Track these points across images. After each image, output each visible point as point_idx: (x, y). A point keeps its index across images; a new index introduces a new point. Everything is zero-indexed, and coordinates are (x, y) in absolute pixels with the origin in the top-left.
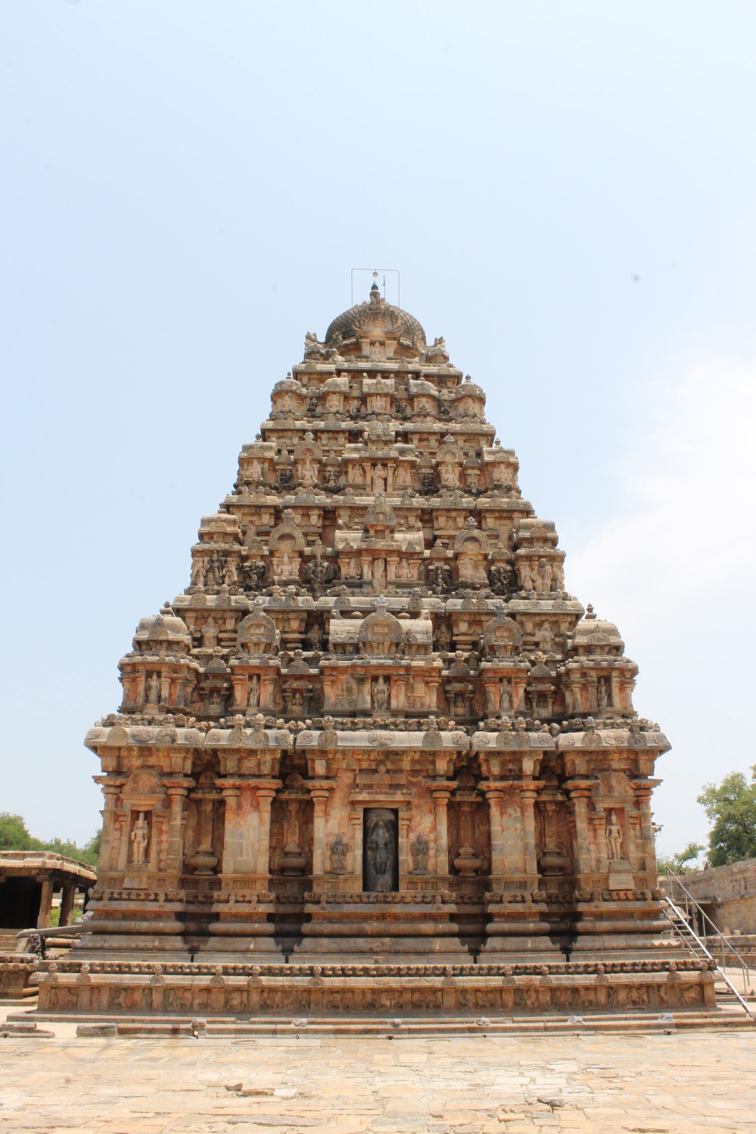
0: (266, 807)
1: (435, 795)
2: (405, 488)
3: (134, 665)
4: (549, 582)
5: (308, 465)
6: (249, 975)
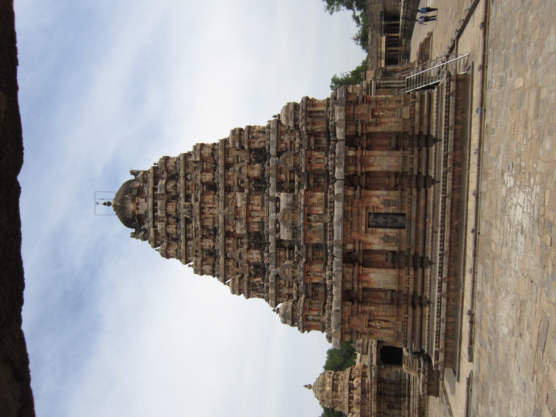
0: (367, 270)
1: (363, 195)
2: (214, 198)
3: (303, 327)
4: (261, 135)
5: (204, 244)
6: (442, 281)
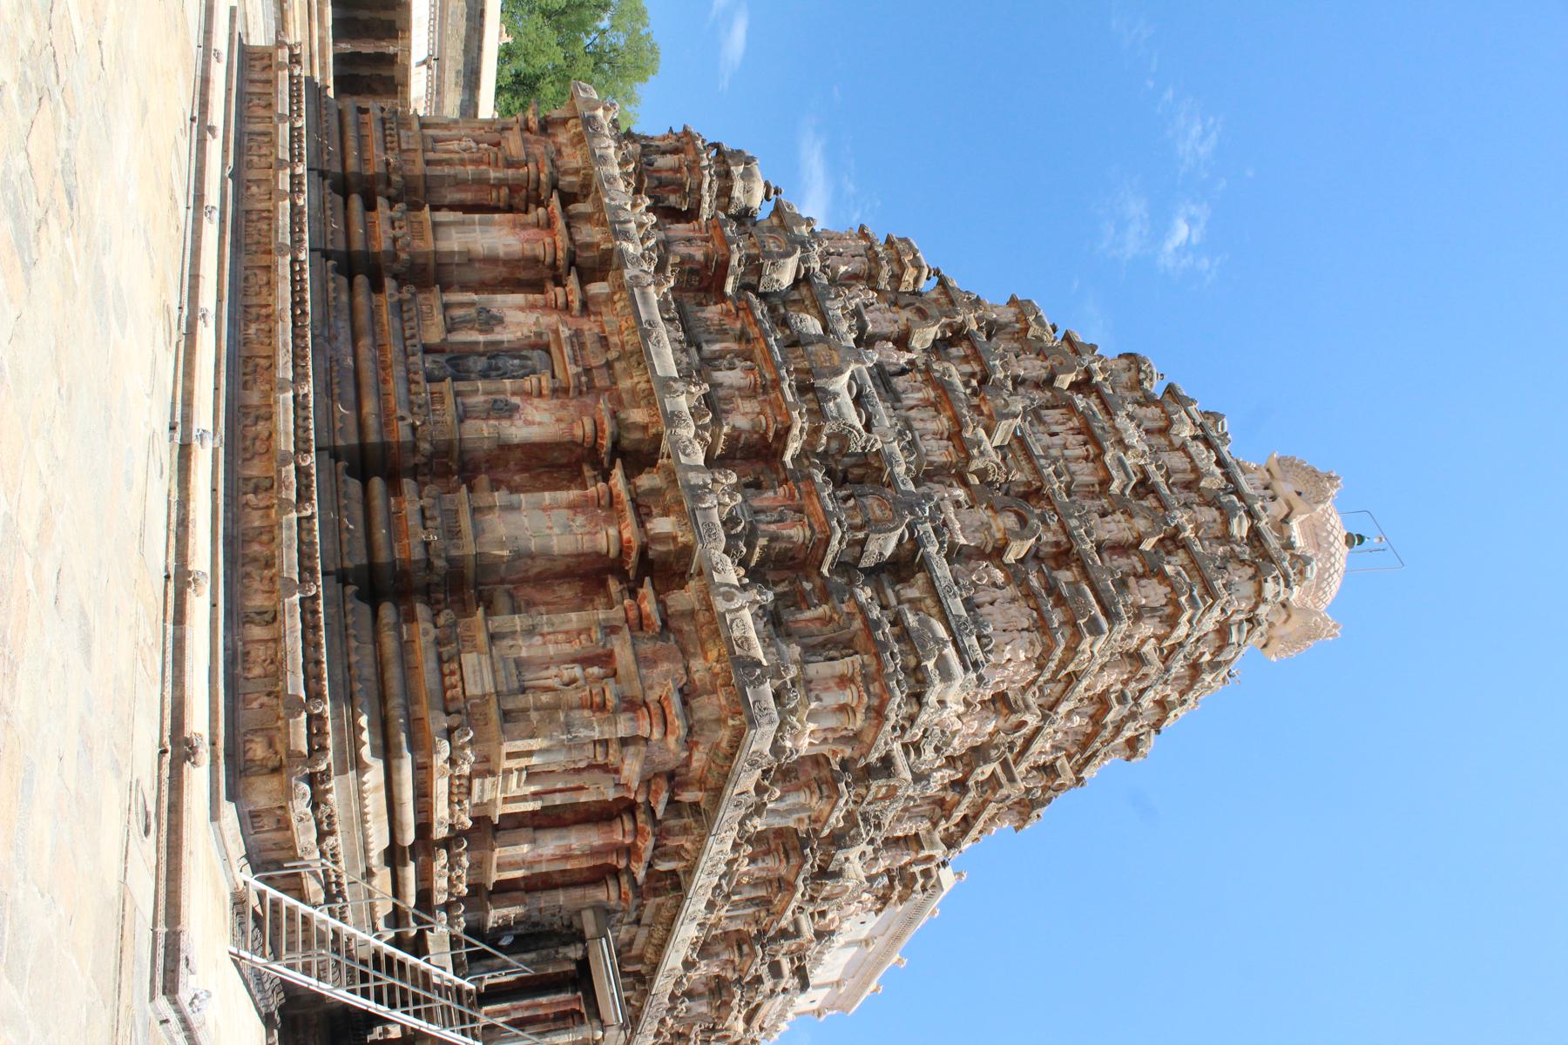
0: (528, 249)
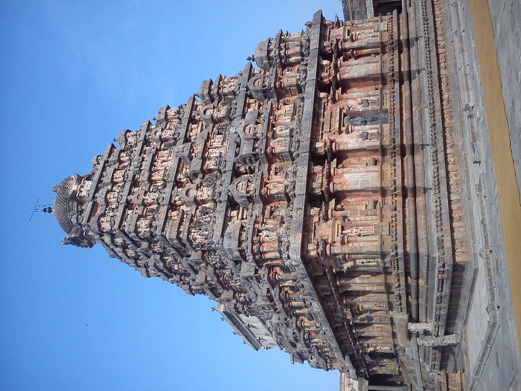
5: (146, 197)
